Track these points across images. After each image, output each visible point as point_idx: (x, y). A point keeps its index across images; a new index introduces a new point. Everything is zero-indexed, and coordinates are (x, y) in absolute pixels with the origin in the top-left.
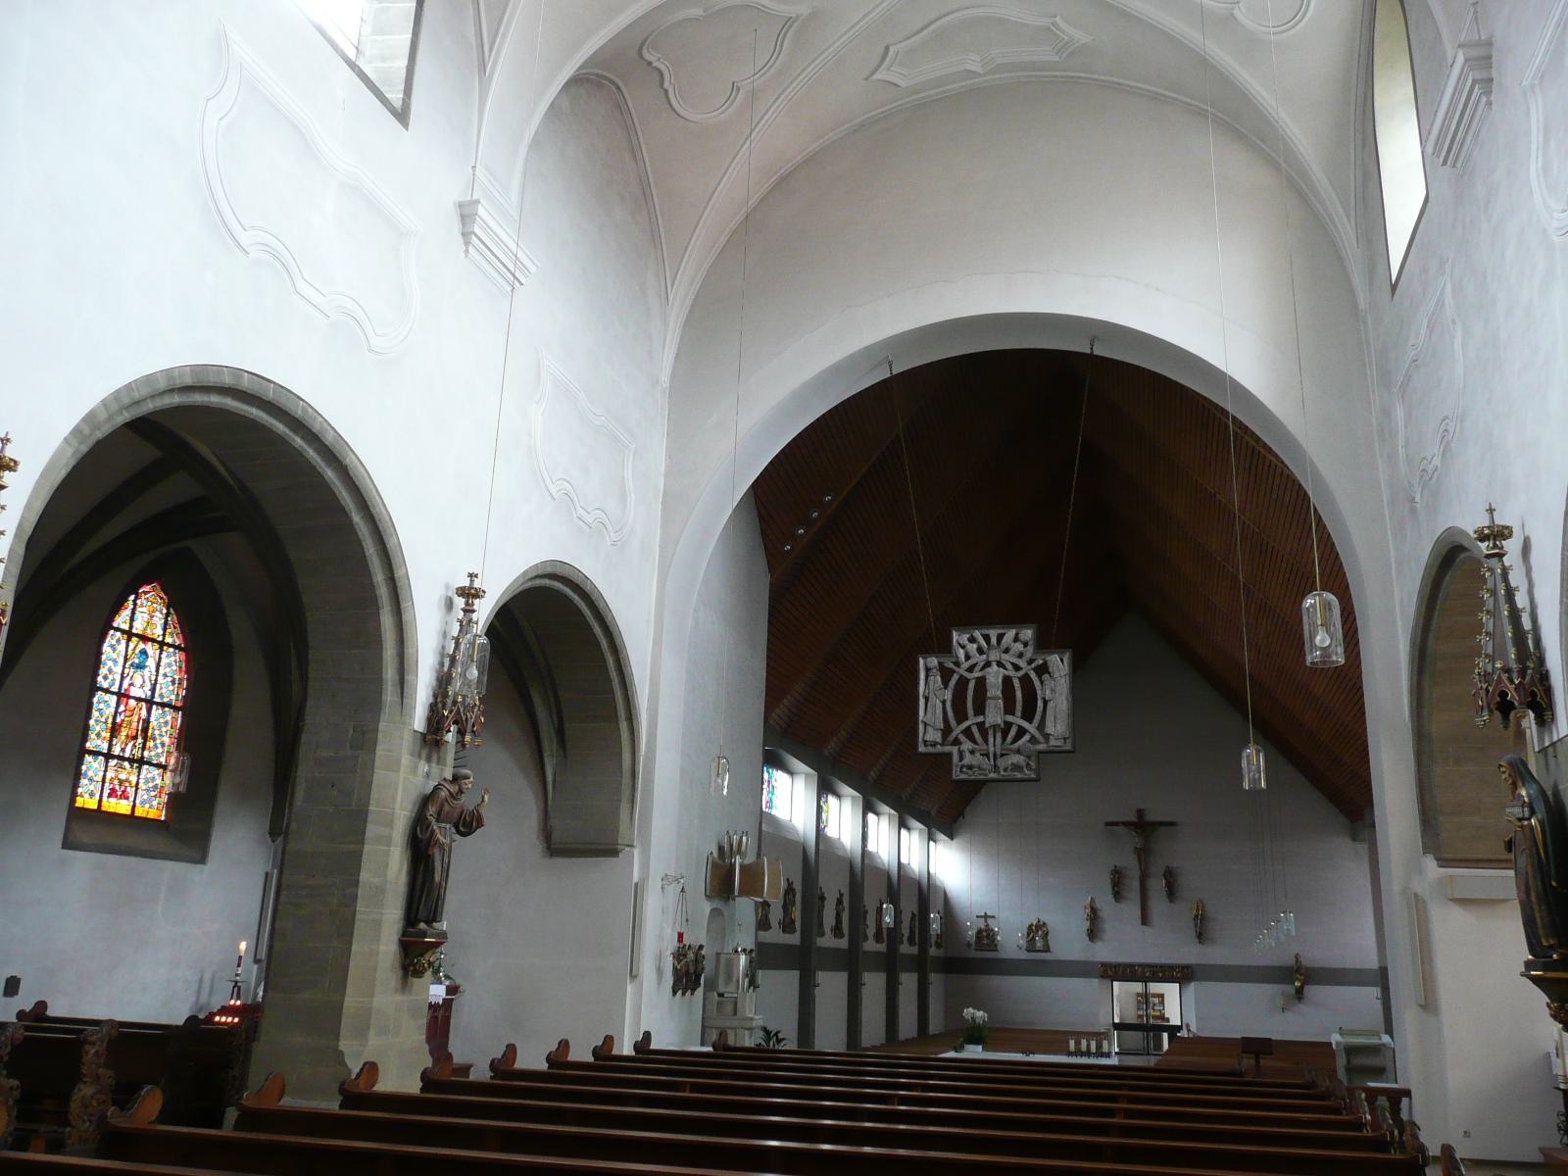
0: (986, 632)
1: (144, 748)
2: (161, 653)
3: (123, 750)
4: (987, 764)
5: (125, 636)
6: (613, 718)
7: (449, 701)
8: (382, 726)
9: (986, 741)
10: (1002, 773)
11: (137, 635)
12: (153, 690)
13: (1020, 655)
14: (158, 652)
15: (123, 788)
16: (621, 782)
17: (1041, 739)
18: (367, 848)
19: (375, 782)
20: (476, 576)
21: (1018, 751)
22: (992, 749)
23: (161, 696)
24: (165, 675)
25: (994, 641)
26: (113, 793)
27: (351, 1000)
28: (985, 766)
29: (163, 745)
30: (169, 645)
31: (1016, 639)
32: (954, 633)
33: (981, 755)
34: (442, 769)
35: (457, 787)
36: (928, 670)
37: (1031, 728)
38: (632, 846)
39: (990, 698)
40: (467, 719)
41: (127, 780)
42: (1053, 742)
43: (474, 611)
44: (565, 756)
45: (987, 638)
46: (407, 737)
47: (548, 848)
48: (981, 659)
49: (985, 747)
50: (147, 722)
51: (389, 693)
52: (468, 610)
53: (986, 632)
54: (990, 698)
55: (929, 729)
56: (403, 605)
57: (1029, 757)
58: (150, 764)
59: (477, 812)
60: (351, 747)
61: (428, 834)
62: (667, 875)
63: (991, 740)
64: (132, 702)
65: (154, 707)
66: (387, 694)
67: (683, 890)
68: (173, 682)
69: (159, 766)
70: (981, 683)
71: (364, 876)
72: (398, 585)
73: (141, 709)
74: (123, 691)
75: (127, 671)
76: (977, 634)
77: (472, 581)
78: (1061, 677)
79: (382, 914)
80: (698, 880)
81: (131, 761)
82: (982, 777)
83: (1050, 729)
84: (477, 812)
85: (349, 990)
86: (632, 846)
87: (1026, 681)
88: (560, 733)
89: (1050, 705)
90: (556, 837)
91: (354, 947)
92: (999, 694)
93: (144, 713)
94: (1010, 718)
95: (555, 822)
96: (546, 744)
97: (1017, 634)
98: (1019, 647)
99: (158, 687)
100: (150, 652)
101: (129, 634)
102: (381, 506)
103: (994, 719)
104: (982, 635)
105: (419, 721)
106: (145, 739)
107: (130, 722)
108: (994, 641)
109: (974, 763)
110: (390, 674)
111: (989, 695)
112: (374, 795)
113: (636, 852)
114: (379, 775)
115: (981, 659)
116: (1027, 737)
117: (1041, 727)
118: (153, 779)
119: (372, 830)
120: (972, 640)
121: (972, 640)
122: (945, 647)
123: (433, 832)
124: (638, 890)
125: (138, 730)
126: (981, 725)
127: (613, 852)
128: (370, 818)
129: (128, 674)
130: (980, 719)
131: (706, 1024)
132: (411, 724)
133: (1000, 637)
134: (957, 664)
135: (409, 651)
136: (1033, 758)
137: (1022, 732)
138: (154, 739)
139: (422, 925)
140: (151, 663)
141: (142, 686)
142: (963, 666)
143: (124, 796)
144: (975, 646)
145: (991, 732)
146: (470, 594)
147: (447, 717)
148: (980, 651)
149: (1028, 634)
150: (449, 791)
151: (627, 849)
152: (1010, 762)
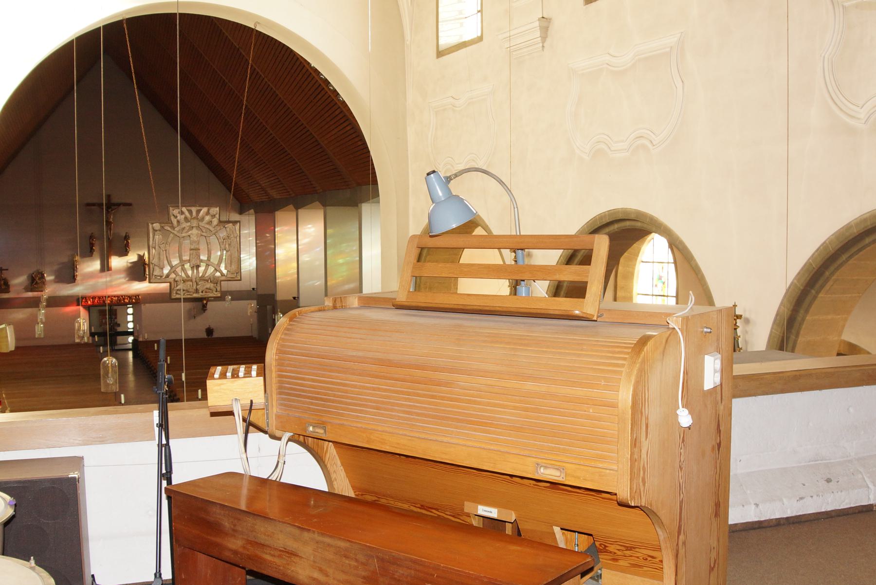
0: (189, 208)
10: (201, 294)
13: (210, 223)
25: (194, 214)
28: (191, 290)
31: (208, 213)
36: (155, 230)
45: (190, 212)
76: (184, 209)
78: (234, 237)
82: (189, 296)
97: (209, 210)
98: (207, 218)
103: (196, 262)
104: (187, 210)
108: (194, 214)
120: (182, 213)
121: (182, 213)
133: (198, 212)
134: (173, 228)
142: (176, 229)
144: (183, 216)
148: (186, 219)
149: (218, 209)
152: (205, 287)
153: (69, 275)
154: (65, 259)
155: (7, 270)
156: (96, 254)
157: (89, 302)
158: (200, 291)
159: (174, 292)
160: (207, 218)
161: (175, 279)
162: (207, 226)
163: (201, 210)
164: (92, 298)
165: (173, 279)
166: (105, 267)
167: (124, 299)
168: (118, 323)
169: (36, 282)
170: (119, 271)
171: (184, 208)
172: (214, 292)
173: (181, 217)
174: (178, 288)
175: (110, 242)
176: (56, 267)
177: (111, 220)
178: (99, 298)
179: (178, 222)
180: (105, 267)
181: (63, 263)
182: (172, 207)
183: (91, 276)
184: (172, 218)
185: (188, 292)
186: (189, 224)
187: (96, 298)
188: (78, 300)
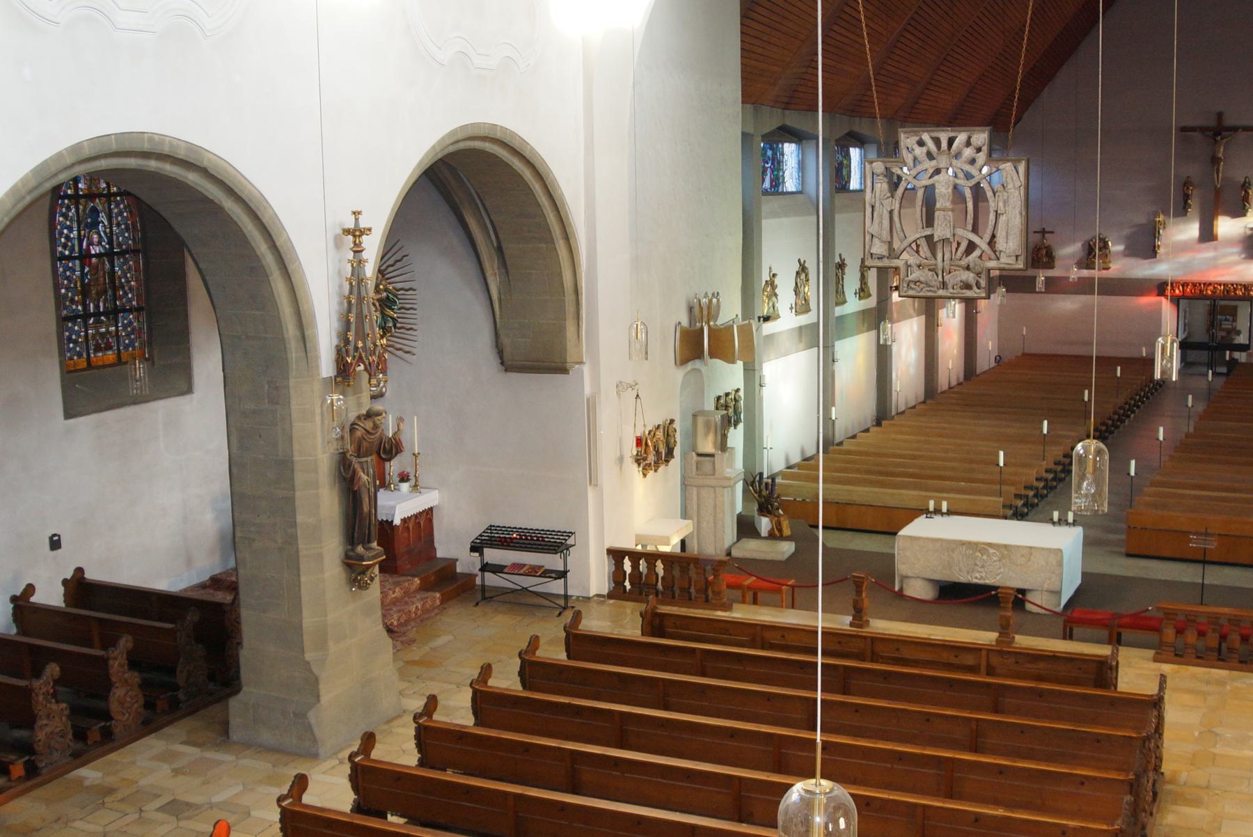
0: (935, 134)
1: (115, 297)
2: (110, 205)
3: (97, 307)
4: (936, 280)
5: (73, 201)
6: (550, 240)
7: (351, 348)
8: (292, 382)
9: (934, 255)
10: (951, 290)
11: (82, 196)
12: (110, 242)
13: (973, 162)
14: (106, 205)
15: (105, 341)
16: (564, 300)
17: (993, 256)
18: (298, 494)
19: (295, 435)
20: (359, 213)
21: (968, 268)
22: (940, 264)
23: (120, 245)
24: (118, 225)
25: (944, 145)
26: (98, 348)
27: (309, 620)
28: (933, 283)
29: (131, 289)
30: (115, 195)
31: (968, 144)
32: (902, 136)
33: (929, 270)
34: (359, 398)
35: (371, 425)
37: (982, 243)
38: (581, 363)
39: (940, 210)
40: (370, 364)
41: (108, 332)
42: (1004, 259)
43: (361, 251)
44: (507, 273)
45: (937, 142)
46: (317, 387)
47: (502, 363)
48: (930, 165)
49: (933, 262)
50: (113, 272)
51: (293, 350)
52: (358, 250)
53: (935, 134)
54: (940, 210)
55: (876, 240)
56: (291, 268)
57: (978, 274)
58: (124, 310)
59: (395, 439)
60: (269, 402)
61: (351, 471)
62: (621, 382)
63: (939, 256)
64: (94, 260)
65: (116, 257)
66: (291, 352)
67: (638, 396)
68: (127, 229)
69: (130, 311)
70: (930, 191)
71: (300, 518)
72: (281, 252)
73: (104, 263)
74: (84, 253)
75: (82, 233)
76: (926, 137)
77: (357, 220)
78: (1014, 188)
79: (321, 548)
80: (666, 347)
81: (106, 313)
83: (1001, 244)
84: (395, 439)
85: (305, 613)
86: (581, 363)
87: (977, 191)
88: (500, 250)
89: (1002, 219)
90: (507, 354)
91: (303, 579)
92: (948, 205)
93: (107, 266)
94: (960, 231)
95: (506, 341)
96: (487, 265)
97: (969, 138)
98: (968, 152)
99: (115, 237)
100: (100, 208)
101: (76, 198)
102: (249, 186)
103: (943, 232)
104: (932, 138)
105: (326, 367)
106: (115, 289)
107: (97, 279)
108: (944, 145)
109: (922, 279)
110: (291, 330)
111: (938, 205)
112: (296, 447)
113: (586, 369)
114: (298, 427)
115: (930, 165)
116: (977, 253)
117: (992, 243)
118: (130, 323)
119: (299, 478)
120: (921, 143)
121: (921, 143)
122: (891, 149)
123: (354, 471)
124: (592, 405)
125: (105, 283)
126: (929, 239)
127: (561, 369)
128: (297, 467)
129: (85, 236)
130: (928, 232)
131: (686, 483)
132: (318, 375)
133: (951, 141)
135: (304, 307)
136: (983, 276)
137: (971, 247)
138: (122, 287)
139: (360, 549)
140: (103, 218)
141: (99, 243)
143: (109, 347)
144: (924, 150)
145: (939, 246)
146: (357, 233)
147: (351, 363)
148: (930, 156)
150: (365, 429)
151: (577, 366)
152: (959, 279)
153: (1146, 245)
154: (1141, 219)
155: (1052, 232)
156: (1193, 211)
157: (1177, 291)
158: (950, 286)
159: (906, 285)
160: (968, 152)
161: (906, 263)
162: (967, 168)
163: (956, 137)
164: (1183, 286)
165: (904, 262)
166: (1207, 234)
167: (1235, 289)
168: (1238, 329)
169: (1093, 253)
170: (1230, 242)
171: (926, 134)
172: (975, 288)
173: (920, 152)
174: (910, 278)
175: (1217, 192)
176: (1126, 232)
177: (1220, 155)
178: (1194, 285)
179: (915, 159)
180: (1207, 234)
181: (1140, 225)
182: (905, 133)
183: (1184, 247)
184: (904, 152)
185: (930, 286)
186: (934, 163)
187: (1188, 285)
188: (1161, 287)
